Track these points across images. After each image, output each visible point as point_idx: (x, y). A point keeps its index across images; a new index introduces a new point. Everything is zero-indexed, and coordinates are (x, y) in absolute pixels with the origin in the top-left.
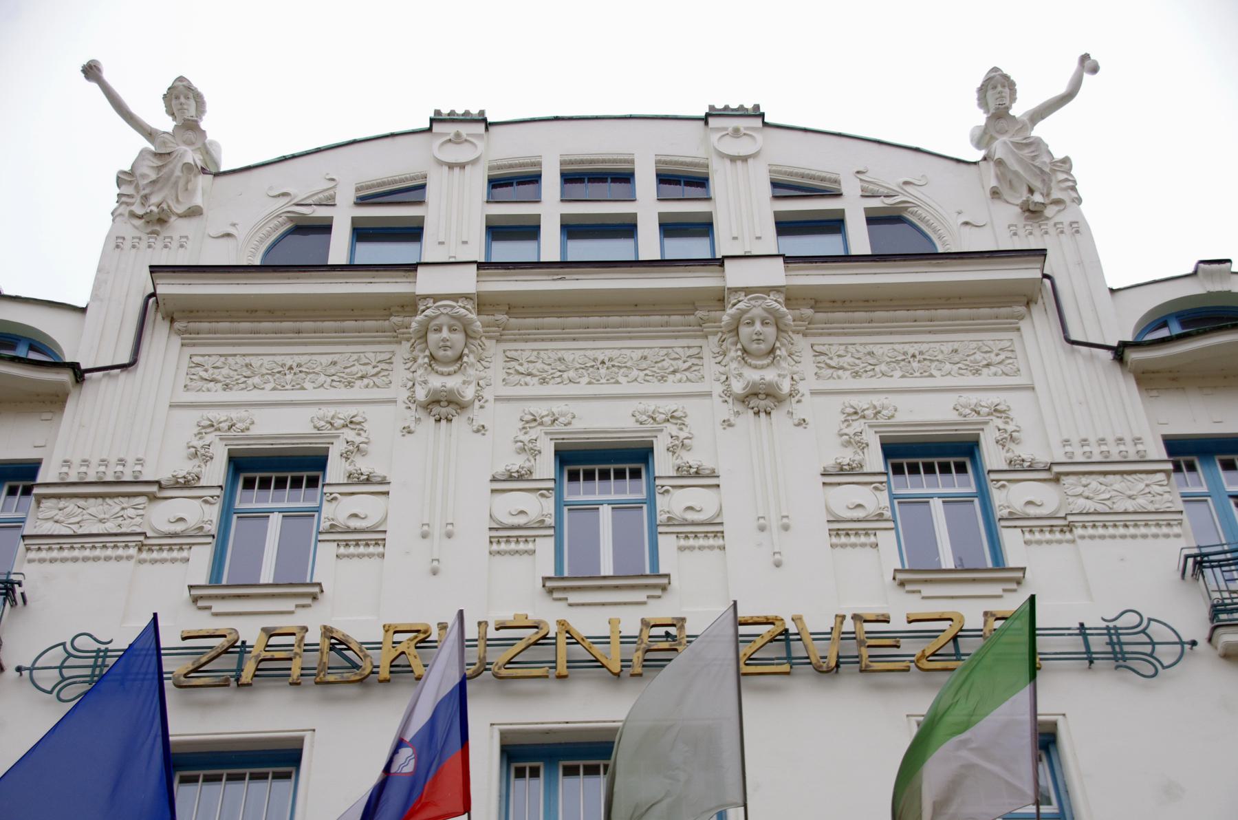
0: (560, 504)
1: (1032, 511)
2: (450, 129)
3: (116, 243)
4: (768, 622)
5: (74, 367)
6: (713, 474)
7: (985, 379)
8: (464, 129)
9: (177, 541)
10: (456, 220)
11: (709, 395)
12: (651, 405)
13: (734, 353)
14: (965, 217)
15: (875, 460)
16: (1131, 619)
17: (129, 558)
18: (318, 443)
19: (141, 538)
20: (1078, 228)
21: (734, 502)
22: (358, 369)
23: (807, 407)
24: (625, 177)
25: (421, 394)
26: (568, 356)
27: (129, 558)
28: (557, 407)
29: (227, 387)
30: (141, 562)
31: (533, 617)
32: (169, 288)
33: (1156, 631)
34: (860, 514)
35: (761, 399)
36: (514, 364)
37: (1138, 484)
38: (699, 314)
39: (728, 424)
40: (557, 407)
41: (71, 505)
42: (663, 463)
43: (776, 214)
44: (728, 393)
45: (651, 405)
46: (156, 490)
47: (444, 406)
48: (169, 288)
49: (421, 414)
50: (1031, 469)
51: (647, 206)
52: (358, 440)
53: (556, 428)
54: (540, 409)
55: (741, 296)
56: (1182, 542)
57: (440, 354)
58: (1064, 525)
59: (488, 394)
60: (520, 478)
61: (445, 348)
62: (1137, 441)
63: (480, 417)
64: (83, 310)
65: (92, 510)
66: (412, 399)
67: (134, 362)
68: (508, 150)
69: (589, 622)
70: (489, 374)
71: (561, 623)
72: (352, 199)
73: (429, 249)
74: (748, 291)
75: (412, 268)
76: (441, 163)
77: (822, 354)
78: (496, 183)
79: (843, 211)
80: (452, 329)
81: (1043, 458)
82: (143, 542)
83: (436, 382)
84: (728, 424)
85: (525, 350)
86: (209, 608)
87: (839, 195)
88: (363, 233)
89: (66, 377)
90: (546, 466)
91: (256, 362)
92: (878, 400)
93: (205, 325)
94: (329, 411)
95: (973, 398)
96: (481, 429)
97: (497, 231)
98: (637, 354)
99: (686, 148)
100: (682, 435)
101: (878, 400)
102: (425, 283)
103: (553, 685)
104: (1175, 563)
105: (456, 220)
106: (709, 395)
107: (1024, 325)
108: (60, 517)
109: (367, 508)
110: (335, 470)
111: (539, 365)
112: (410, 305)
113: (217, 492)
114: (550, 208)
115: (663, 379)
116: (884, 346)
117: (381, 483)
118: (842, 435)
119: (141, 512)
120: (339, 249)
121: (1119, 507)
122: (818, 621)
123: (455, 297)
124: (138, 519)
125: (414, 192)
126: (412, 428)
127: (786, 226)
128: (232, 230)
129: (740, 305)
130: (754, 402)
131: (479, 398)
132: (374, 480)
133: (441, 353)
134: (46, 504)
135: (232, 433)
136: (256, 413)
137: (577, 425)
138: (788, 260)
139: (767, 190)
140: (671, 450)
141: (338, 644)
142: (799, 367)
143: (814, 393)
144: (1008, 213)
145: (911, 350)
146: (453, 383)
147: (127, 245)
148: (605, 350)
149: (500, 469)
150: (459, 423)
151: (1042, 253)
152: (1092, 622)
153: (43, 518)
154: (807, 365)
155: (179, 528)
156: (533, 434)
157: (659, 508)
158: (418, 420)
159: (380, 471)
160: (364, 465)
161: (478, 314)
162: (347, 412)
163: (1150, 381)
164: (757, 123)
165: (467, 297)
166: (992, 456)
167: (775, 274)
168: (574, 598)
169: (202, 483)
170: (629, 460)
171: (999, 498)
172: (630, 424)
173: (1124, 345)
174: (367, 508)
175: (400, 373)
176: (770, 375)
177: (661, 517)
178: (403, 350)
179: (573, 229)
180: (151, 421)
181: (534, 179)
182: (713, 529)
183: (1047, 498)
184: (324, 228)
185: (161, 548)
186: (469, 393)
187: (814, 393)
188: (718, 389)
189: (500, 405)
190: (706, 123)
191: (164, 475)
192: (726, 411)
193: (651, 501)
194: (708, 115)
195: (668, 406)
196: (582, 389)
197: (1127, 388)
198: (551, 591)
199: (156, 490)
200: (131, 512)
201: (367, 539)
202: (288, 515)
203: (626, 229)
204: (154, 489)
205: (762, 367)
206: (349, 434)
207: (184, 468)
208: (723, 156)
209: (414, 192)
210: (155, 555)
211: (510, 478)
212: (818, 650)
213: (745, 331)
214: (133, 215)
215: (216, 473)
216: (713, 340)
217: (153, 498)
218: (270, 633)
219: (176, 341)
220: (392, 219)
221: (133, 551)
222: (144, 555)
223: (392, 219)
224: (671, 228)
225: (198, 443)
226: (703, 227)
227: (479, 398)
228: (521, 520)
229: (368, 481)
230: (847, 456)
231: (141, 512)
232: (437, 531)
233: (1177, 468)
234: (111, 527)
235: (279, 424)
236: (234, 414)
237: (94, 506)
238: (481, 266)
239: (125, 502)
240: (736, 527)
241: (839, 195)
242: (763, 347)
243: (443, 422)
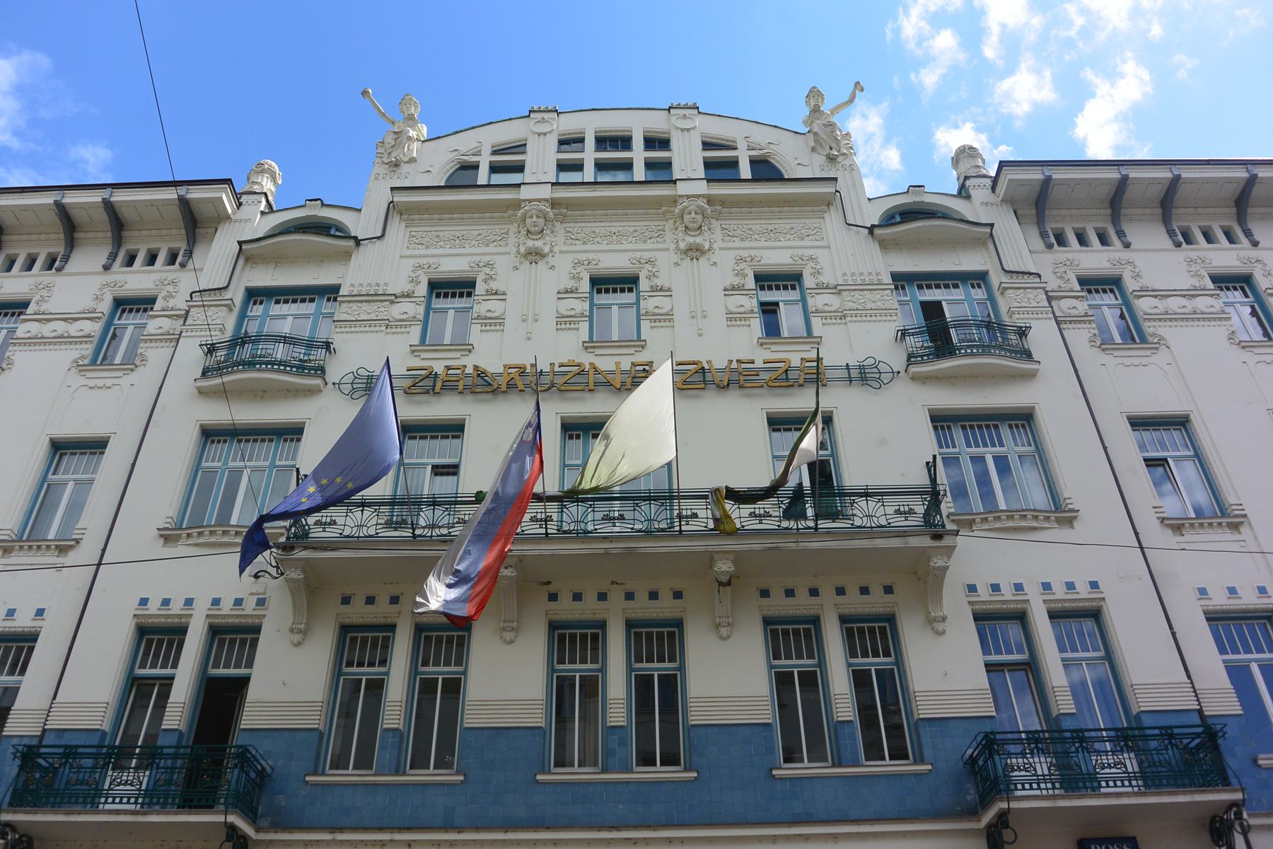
0: (592, 305)
1: (827, 308)
2: (539, 116)
4: (694, 363)
5: (355, 238)
7: (807, 242)
8: (546, 116)
9: (404, 323)
10: (541, 160)
12: (638, 255)
13: (681, 228)
14: (795, 159)
15: (751, 283)
16: (871, 361)
18: (471, 275)
20: (853, 168)
21: (680, 304)
22: (492, 238)
23: (716, 256)
25: (522, 249)
26: (597, 230)
28: (591, 256)
29: (427, 247)
31: (577, 361)
32: (400, 198)
33: (882, 367)
34: (742, 310)
35: (695, 252)
37: (877, 295)
39: (677, 264)
40: (591, 256)
41: (354, 306)
42: (644, 284)
44: (677, 248)
45: (638, 255)
46: (395, 298)
47: (535, 256)
48: (400, 198)
50: (827, 288)
51: (638, 154)
56: (896, 324)
57: (532, 229)
58: (841, 315)
59: (556, 249)
60: (572, 292)
62: (878, 274)
64: (360, 210)
66: (518, 252)
67: (383, 235)
68: (568, 124)
69: (605, 364)
70: (555, 239)
71: (591, 364)
73: (528, 176)
74: (688, 197)
75: (519, 185)
78: (562, 142)
80: (538, 217)
81: (833, 282)
83: (530, 243)
84: (677, 264)
85: (575, 227)
87: (736, 149)
88: (495, 169)
89: (351, 243)
90: (585, 286)
91: (441, 234)
92: (752, 253)
94: (478, 258)
95: (800, 252)
96: (553, 267)
98: (632, 229)
99: (657, 123)
101: (752, 253)
102: (525, 193)
103: (588, 395)
104: (893, 334)
105: (541, 160)
107: (826, 216)
109: (495, 306)
110: (480, 288)
112: (517, 204)
114: (589, 155)
115: (645, 242)
116: (757, 225)
120: (483, 176)
121: (868, 307)
122: (720, 363)
123: (539, 200)
125: (520, 147)
127: (708, 164)
130: (690, 253)
131: (551, 251)
134: (344, 305)
137: (601, 265)
138: (709, 181)
139: (700, 146)
140: (648, 278)
141: (480, 373)
142: (713, 236)
143: (721, 249)
144: (819, 159)
145: (770, 228)
146: (539, 244)
148: (616, 227)
149: (562, 288)
150: (542, 264)
151: (835, 179)
152: (852, 363)
153: (343, 311)
154: (718, 235)
155: (404, 317)
159: (502, 289)
160: (494, 286)
162: (485, 259)
163: (884, 245)
164: (695, 112)
165: (546, 200)
166: (808, 281)
167: (702, 188)
168: (598, 351)
170: (627, 283)
171: (810, 302)
172: (628, 264)
173: (873, 226)
174: (495, 306)
175: (512, 239)
176: (699, 240)
177: (643, 312)
178: (514, 228)
179: (601, 166)
180: (391, 264)
181: (582, 140)
182: (668, 317)
183: (833, 301)
184: (475, 167)
186: (547, 249)
187: (721, 249)
188: (673, 246)
191: (398, 291)
192: (676, 258)
193: (638, 303)
195: (647, 255)
197: (875, 247)
198: (587, 348)
199: (395, 298)
201: (494, 322)
202: (457, 310)
206: (487, 270)
207: (407, 287)
208: (677, 128)
209: (520, 147)
211: (567, 292)
212: (718, 377)
213: (686, 217)
215: (422, 289)
216: (671, 222)
217: (392, 302)
219: (403, 225)
220: (509, 162)
223: (509, 162)
224: (650, 165)
227: (551, 251)
228: (572, 313)
229: (496, 294)
230: (737, 281)
233: (897, 288)
235: (453, 266)
236: (431, 260)
237: (365, 306)
238: (553, 184)
240: (680, 315)
242: (695, 225)
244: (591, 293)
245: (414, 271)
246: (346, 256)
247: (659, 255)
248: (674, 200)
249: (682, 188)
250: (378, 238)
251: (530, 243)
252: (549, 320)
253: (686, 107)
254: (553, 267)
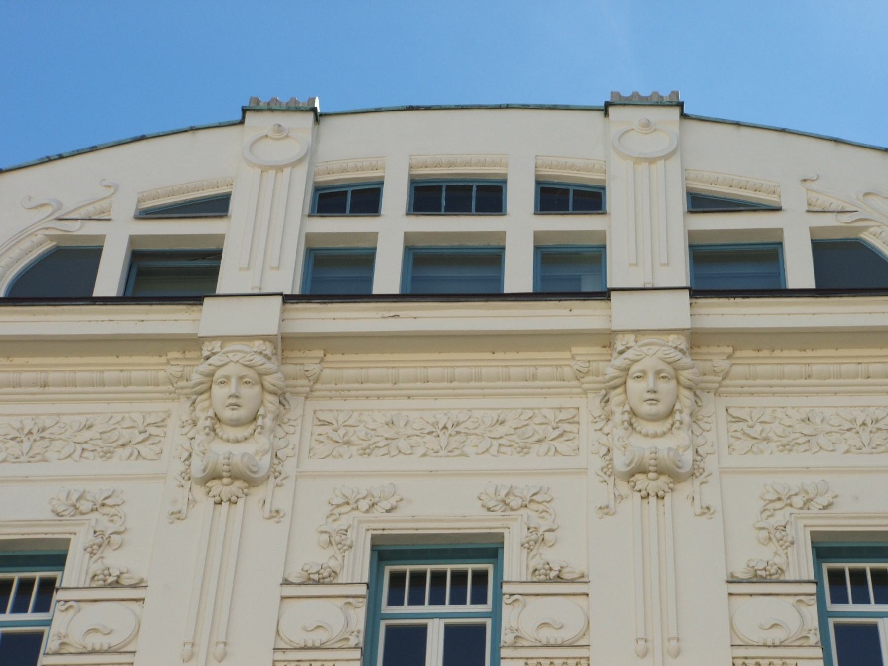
6: (581, 579)
18: (54, 532)
25: (197, 467)
36: (328, 429)
39: (605, 510)
43: (691, 234)
44: (608, 470)
55: (631, 338)
57: (227, 414)
77: (739, 420)
79: (781, 231)
84: (605, 510)
96: (276, 514)
100: (544, 525)
115: (524, 450)
117: (134, 586)
129: (629, 354)
132: (124, 581)
138: (696, 293)
139: (679, 203)
157: (504, 624)
159: (139, 572)
160: (114, 561)
167: (677, 310)
188: (598, 463)
190: (606, 114)
194: (608, 105)
205: (655, 436)
238: (287, 299)
241: (779, 209)
243: (225, 505)
244: (373, 586)
248: (606, 339)
249: (622, 312)
253: (657, 102)
254: (276, 514)
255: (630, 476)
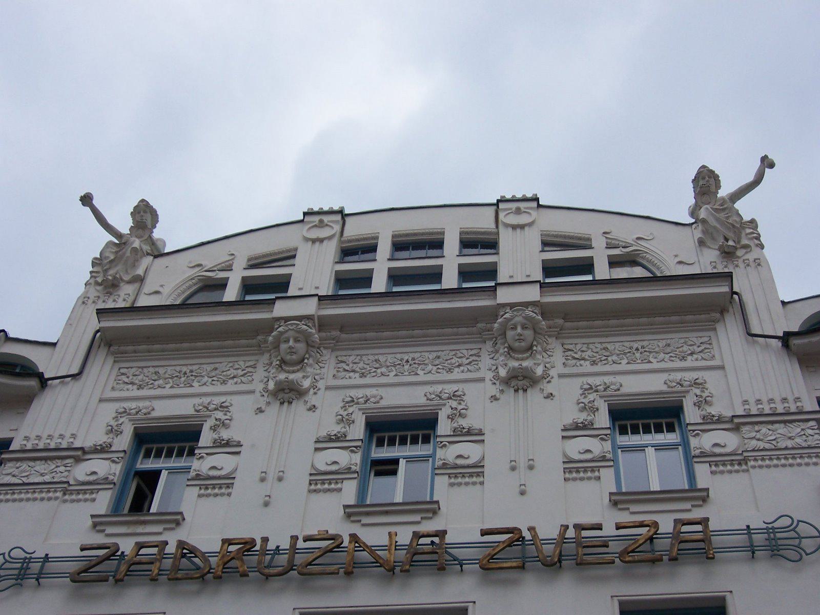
3: (84, 300)
9: (92, 486)
11: (482, 380)
17: (56, 498)
19: (66, 485)
22: (232, 372)
24: (435, 244)
26: (382, 359)
27: (56, 498)
28: (369, 392)
29: (140, 387)
30: (65, 501)
31: (332, 532)
38: (479, 325)
39: (494, 398)
41: (24, 466)
45: (438, 388)
47: (287, 394)
49: (270, 399)
52: (224, 417)
53: (367, 405)
54: (357, 393)
59: (321, 384)
61: (292, 353)
63: (312, 399)
64: (54, 345)
65: (37, 468)
67: (80, 373)
72: (244, 265)
76: (307, 239)
80: (297, 340)
82: (67, 489)
83: (282, 376)
84: (494, 398)
86: (103, 531)
91: (161, 371)
92: (608, 379)
93: (130, 348)
97: (342, 280)
99: (483, 222)
101: (608, 379)
106: (482, 380)
108: (16, 472)
111: (361, 365)
113: (122, 455)
118: (579, 404)
119: (68, 469)
124: (66, 474)
126: (263, 408)
128: (161, 289)
130: (514, 383)
133: (288, 357)
135: (139, 416)
136: (156, 404)
137: (383, 403)
140: (451, 418)
143: (561, 376)
145: (635, 345)
147: (90, 301)
149: (323, 433)
154: (558, 357)
156: (350, 410)
158: (268, 403)
161: (320, 331)
168: (366, 520)
169: (113, 449)
172: (423, 401)
175: (260, 373)
178: (265, 358)
185: (78, 492)
186: (306, 383)
187: (561, 376)
189: (328, 393)
196: (392, 379)
200: (62, 469)
203: (435, 275)
204: (79, 453)
206: (219, 415)
210: (74, 497)
213: (510, 334)
214: (97, 283)
218: (140, 546)
221: (59, 494)
222: (67, 497)
224: (466, 273)
225: (114, 423)
226: (490, 272)
227: (314, 387)
231: (68, 469)
232: (271, 476)
234: (47, 478)
237: (40, 467)
239: (59, 462)
245: (116, 418)
246: (24, 402)
247: (469, 388)
250: (74, 376)
251: (282, 376)
252: (299, 478)
255: (507, 381)
